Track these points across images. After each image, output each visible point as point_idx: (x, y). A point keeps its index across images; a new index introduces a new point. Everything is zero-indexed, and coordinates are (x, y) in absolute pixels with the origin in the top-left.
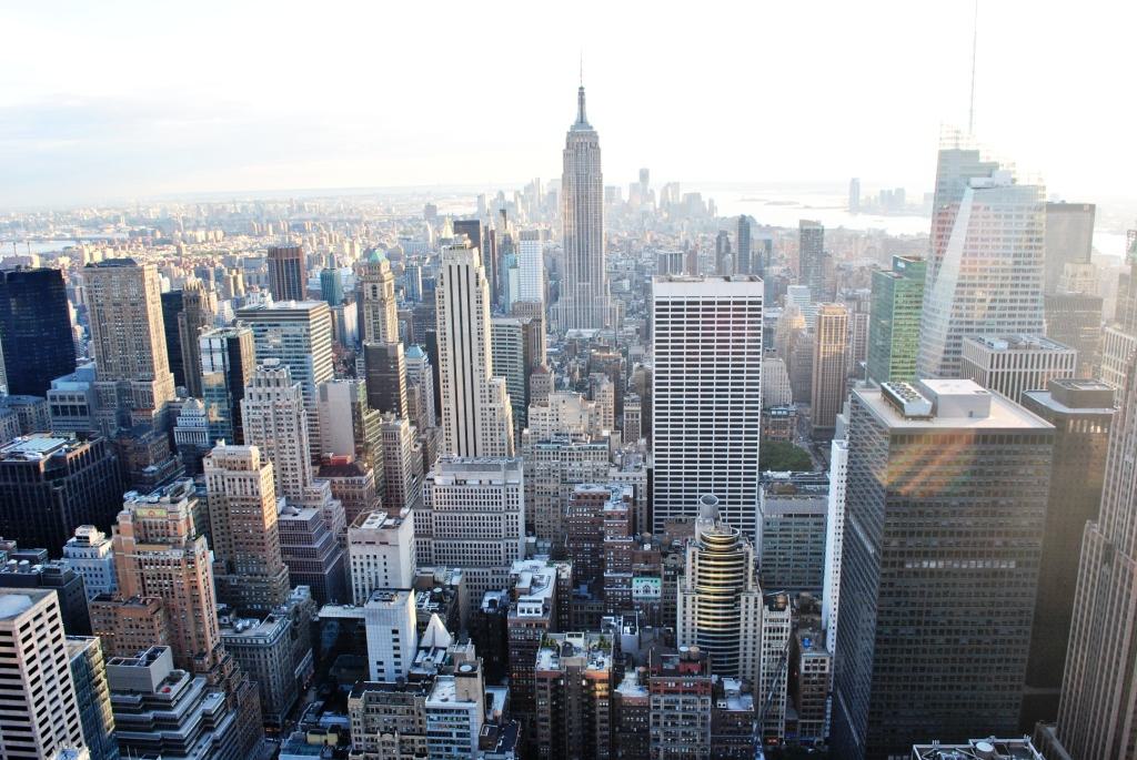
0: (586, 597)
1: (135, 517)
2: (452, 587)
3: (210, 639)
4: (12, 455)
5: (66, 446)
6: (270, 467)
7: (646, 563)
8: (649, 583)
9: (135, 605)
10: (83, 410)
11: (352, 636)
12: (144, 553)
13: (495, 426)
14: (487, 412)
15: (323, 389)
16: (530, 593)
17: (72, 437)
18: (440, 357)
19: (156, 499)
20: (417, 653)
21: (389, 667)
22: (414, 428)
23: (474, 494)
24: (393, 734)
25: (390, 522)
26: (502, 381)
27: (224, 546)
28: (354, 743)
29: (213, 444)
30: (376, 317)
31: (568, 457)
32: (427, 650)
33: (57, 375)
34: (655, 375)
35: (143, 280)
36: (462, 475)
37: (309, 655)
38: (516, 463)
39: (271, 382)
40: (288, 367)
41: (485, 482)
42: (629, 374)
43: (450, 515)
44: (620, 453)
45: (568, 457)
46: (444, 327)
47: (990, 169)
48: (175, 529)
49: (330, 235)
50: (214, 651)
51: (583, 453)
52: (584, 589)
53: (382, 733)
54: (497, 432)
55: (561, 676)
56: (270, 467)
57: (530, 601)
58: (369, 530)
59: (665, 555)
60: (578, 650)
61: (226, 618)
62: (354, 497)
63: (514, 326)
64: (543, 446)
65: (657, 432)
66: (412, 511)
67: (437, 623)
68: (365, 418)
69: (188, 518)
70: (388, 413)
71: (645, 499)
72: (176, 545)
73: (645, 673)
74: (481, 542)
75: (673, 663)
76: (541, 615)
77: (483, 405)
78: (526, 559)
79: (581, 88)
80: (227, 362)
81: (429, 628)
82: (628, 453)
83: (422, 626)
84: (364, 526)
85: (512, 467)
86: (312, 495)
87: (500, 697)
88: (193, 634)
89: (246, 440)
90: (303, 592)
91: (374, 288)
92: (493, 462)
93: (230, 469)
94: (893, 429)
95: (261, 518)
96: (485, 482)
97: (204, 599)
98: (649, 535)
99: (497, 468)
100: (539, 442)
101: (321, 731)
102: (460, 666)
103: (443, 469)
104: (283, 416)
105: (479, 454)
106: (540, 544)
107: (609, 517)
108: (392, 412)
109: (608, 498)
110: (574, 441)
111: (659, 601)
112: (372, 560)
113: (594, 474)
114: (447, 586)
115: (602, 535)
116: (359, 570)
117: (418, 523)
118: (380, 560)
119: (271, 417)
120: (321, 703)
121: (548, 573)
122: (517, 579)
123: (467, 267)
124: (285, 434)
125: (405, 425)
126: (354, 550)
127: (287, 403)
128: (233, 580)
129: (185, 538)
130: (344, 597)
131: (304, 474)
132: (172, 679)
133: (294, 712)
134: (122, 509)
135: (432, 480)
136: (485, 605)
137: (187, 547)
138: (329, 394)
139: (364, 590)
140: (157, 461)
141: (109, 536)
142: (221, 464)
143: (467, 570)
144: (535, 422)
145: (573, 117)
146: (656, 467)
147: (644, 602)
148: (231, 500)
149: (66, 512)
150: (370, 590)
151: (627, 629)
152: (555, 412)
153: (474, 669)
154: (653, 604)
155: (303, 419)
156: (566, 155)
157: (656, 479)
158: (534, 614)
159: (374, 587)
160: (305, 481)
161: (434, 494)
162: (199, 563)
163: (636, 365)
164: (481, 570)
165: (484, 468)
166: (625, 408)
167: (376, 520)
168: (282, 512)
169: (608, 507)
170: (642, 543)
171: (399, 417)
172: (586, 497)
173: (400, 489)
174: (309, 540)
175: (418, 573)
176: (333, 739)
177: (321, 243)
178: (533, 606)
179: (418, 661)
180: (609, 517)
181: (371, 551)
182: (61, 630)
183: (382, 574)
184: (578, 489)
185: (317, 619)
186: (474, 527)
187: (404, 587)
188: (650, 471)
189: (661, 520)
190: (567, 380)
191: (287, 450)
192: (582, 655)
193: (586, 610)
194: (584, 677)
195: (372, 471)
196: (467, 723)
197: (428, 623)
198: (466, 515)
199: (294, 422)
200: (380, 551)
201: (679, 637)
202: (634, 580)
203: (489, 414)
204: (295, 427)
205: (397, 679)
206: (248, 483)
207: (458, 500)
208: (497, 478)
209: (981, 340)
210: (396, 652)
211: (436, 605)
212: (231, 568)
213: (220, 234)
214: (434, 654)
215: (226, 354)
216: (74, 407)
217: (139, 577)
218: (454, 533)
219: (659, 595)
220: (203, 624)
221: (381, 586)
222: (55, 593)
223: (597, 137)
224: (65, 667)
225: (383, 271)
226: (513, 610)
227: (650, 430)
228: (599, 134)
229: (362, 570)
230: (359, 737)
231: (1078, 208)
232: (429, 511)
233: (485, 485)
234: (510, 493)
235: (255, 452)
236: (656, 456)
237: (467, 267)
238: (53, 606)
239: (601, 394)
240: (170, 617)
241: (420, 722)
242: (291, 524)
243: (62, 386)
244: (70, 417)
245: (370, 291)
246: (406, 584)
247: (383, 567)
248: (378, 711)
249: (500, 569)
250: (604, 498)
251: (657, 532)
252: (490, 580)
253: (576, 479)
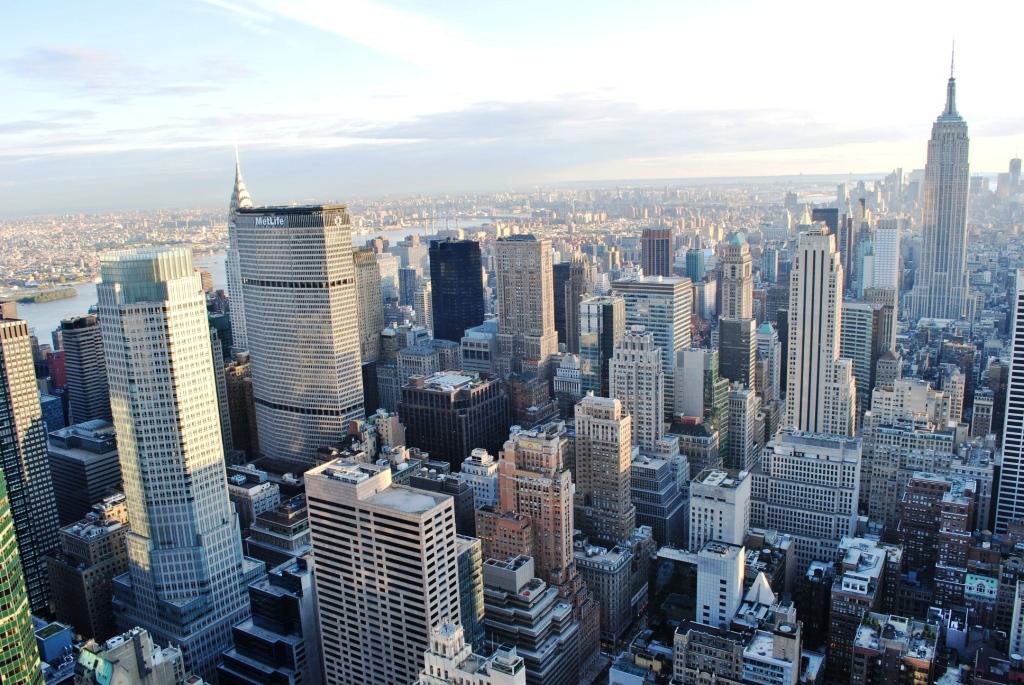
0: (914, 584)
1: (517, 447)
2: (780, 550)
3: (565, 558)
4: (432, 386)
5: (471, 383)
6: (628, 419)
7: (983, 561)
8: (984, 582)
9: (510, 519)
10: (486, 356)
11: (684, 579)
12: (522, 478)
14: (832, 390)
15: (681, 356)
16: (857, 569)
17: (477, 376)
18: (790, 336)
19: (534, 434)
20: (741, 606)
21: (714, 612)
22: (759, 399)
23: (811, 467)
24: (711, 674)
25: (729, 482)
26: (849, 363)
27: (584, 481)
28: (676, 674)
29: (584, 394)
30: (732, 295)
31: (909, 443)
32: (751, 604)
33: (469, 325)
34: (1011, 371)
35: (540, 253)
36: (801, 448)
37: (646, 587)
38: (855, 443)
39: (637, 347)
40: (652, 333)
41: (823, 457)
42: (983, 367)
43: (786, 483)
44: (965, 445)
45: (909, 443)
46: (796, 308)
48: (547, 461)
49: (697, 220)
50: (567, 568)
51: (925, 441)
52: (913, 575)
53: (701, 671)
54: (839, 411)
55: (880, 656)
56: (628, 419)
57: (856, 578)
58: (710, 486)
59: (1006, 556)
60: (900, 634)
61: (580, 542)
62: (699, 455)
63: (867, 312)
64: (885, 430)
65: (1009, 430)
66: (750, 475)
67: (763, 581)
68: (715, 385)
69: (558, 453)
70: (736, 383)
71: (989, 496)
72: (546, 474)
73: (969, 672)
74: (813, 514)
75: (1001, 668)
76: (865, 592)
77: (828, 384)
78: (856, 536)
79: (952, 80)
80: (601, 326)
81: (755, 584)
82: (975, 447)
83: (748, 581)
84: (706, 482)
85: (851, 446)
86: (662, 448)
87: (816, 664)
88: (552, 551)
89: (611, 394)
90: (646, 532)
91: (733, 268)
92: (832, 439)
93: (595, 417)
95: (617, 462)
96: (823, 457)
97: (564, 523)
98: (990, 533)
99: (836, 445)
100: (880, 426)
101: (648, 656)
102: (780, 625)
103: (784, 440)
104: (645, 376)
105: (820, 430)
106: (872, 524)
107: (947, 509)
108: (740, 382)
109: (948, 489)
110: (917, 428)
111: (994, 602)
112: (709, 514)
113: (935, 464)
114: (776, 549)
115: (938, 525)
116: (696, 521)
117: (754, 487)
118: (717, 515)
119: (634, 376)
120: (651, 632)
121: (877, 554)
122: (845, 554)
123: (823, 252)
124: (645, 391)
125: (751, 395)
126: (694, 502)
127: (649, 365)
128: (589, 511)
129: (554, 470)
130: (681, 542)
131: (657, 429)
132: (532, 585)
133: (628, 634)
134: (508, 439)
135: (772, 448)
136: (811, 573)
137: (555, 478)
138: (685, 360)
139: (699, 539)
140: (538, 402)
141: (496, 459)
142: (589, 411)
143: (797, 537)
144: (877, 405)
145: (944, 107)
146: (1005, 466)
147: (976, 600)
148: (594, 443)
149: (467, 435)
150: (705, 540)
151: (955, 624)
152: (900, 399)
153: (794, 631)
154: (986, 604)
155: (660, 380)
156: (931, 146)
157: (1004, 477)
158: (858, 591)
159: (708, 538)
160: (657, 434)
161: (773, 462)
162: (563, 492)
163: (993, 358)
164: (810, 540)
165: (823, 443)
166: (975, 401)
167: (717, 478)
168: (636, 460)
169: (947, 498)
170: (981, 540)
171: (746, 387)
172: (925, 485)
173: (741, 453)
175: (750, 532)
176: (657, 666)
177: (688, 226)
178: (859, 583)
179: (741, 612)
180: (947, 509)
181: (708, 504)
182: (453, 529)
183: (717, 528)
184: (917, 476)
185: (655, 558)
186: (808, 498)
187: (735, 543)
188: (997, 469)
189: (1005, 520)
190: (915, 368)
191: (644, 406)
192: (903, 640)
193: (913, 596)
194: (903, 662)
195: (717, 433)
196: (780, 679)
197: (754, 580)
198: (801, 486)
199: (653, 382)
200: (719, 506)
201: (1012, 644)
202: (968, 577)
203: (833, 394)
204: (653, 387)
205: (722, 626)
206: (610, 429)
207: (795, 471)
208: (836, 455)
210: (723, 601)
211: (764, 564)
212: (588, 500)
213: (604, 216)
214: (757, 609)
215: (601, 318)
216: (479, 352)
217: (515, 497)
218: (788, 501)
219: (994, 596)
220: (561, 544)
221: (715, 539)
222: (452, 499)
223: (966, 128)
224: (453, 559)
225: (742, 253)
226: (837, 582)
227: (1002, 427)
228: (968, 124)
229: (700, 521)
230: (680, 670)
232: (766, 477)
233: (822, 460)
234: (847, 471)
235: (617, 404)
236: (1006, 454)
237: (823, 252)
238: (450, 509)
239: (951, 384)
240: (536, 533)
241: (737, 669)
242: (641, 471)
243: (472, 335)
244: (476, 361)
245: (729, 272)
246: (738, 540)
247: (719, 522)
248: (700, 650)
249: (829, 542)
251: (998, 531)
252: (818, 551)
253: (915, 466)
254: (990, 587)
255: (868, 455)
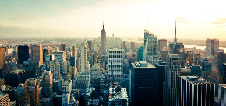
3: (37, 101)
6: (52, 74)
13: (87, 68)
15: (63, 63)
16: (88, 93)
17: (24, 70)
25: (69, 82)
33: (25, 61)
36: (81, 75)
47: (151, 35)
56: (52, 74)
68: (69, 67)
72: (34, 86)
79: (103, 26)
83: (71, 98)
94: (135, 68)
95: (50, 82)
99: (86, 74)
105: (85, 72)
125: (75, 68)
126: (63, 87)
134: (26, 80)
142: (45, 74)
145: (102, 29)
156: (101, 33)
168: (55, 81)
169: (101, 80)
170: (106, 85)
171: (75, 67)
174: (58, 85)
181: (65, 87)
184: (97, 77)
190: (99, 62)
208: (86, 75)
209: (150, 57)
220: (37, 99)
231: (165, 40)
235: (50, 72)
238: (7, 96)
243: (25, 62)
250: (101, 78)
254: (107, 91)
255: (91, 75)
